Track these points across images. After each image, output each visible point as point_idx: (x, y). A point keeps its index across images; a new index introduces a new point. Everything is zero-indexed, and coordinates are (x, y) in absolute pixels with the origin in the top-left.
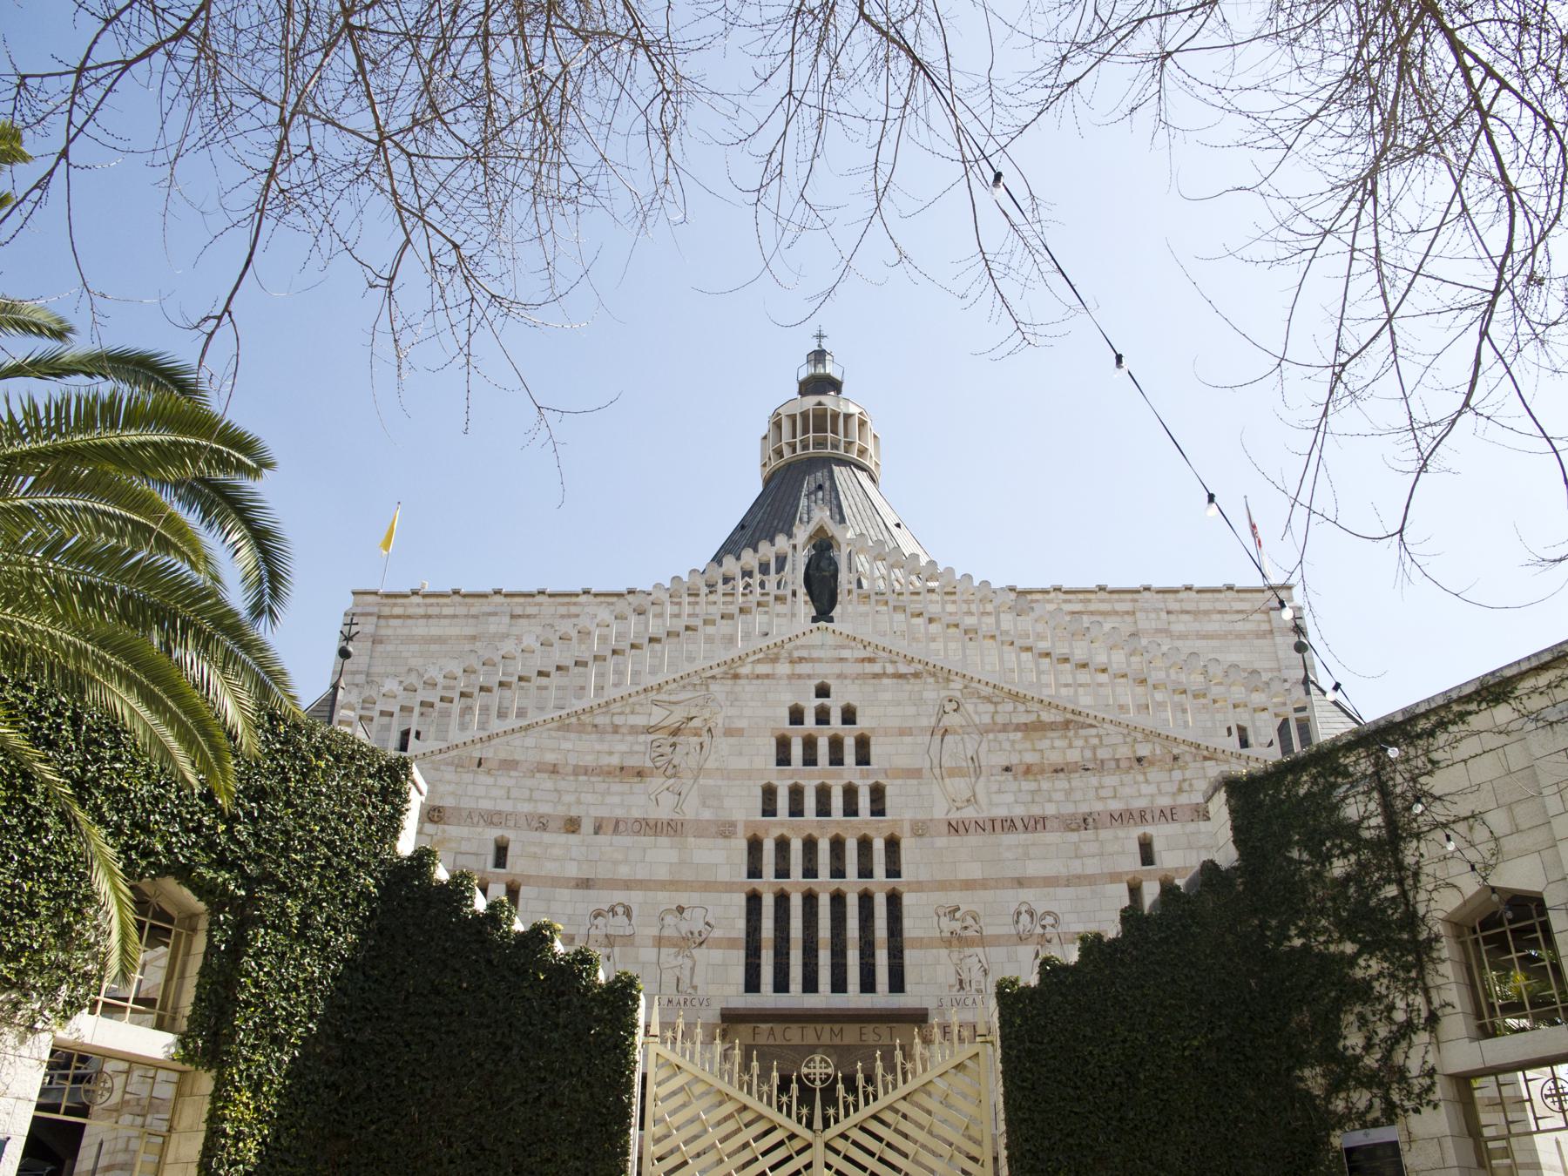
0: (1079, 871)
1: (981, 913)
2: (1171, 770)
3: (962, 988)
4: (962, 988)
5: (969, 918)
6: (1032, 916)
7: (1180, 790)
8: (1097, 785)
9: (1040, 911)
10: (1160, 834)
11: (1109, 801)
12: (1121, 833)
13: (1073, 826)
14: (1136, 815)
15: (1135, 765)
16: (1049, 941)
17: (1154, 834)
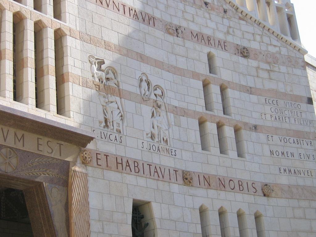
0: (174, 64)
1: (119, 72)
2: (223, 18)
3: (107, 126)
4: (107, 126)
5: (110, 71)
6: (148, 84)
7: (228, 33)
8: (183, 9)
9: (153, 83)
10: (220, 56)
11: (191, 23)
12: (198, 47)
13: (171, 31)
14: (206, 38)
15: (204, 5)
16: (159, 107)
17: (216, 55)
